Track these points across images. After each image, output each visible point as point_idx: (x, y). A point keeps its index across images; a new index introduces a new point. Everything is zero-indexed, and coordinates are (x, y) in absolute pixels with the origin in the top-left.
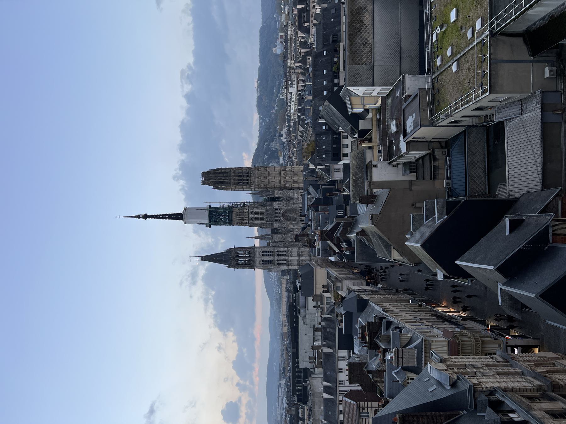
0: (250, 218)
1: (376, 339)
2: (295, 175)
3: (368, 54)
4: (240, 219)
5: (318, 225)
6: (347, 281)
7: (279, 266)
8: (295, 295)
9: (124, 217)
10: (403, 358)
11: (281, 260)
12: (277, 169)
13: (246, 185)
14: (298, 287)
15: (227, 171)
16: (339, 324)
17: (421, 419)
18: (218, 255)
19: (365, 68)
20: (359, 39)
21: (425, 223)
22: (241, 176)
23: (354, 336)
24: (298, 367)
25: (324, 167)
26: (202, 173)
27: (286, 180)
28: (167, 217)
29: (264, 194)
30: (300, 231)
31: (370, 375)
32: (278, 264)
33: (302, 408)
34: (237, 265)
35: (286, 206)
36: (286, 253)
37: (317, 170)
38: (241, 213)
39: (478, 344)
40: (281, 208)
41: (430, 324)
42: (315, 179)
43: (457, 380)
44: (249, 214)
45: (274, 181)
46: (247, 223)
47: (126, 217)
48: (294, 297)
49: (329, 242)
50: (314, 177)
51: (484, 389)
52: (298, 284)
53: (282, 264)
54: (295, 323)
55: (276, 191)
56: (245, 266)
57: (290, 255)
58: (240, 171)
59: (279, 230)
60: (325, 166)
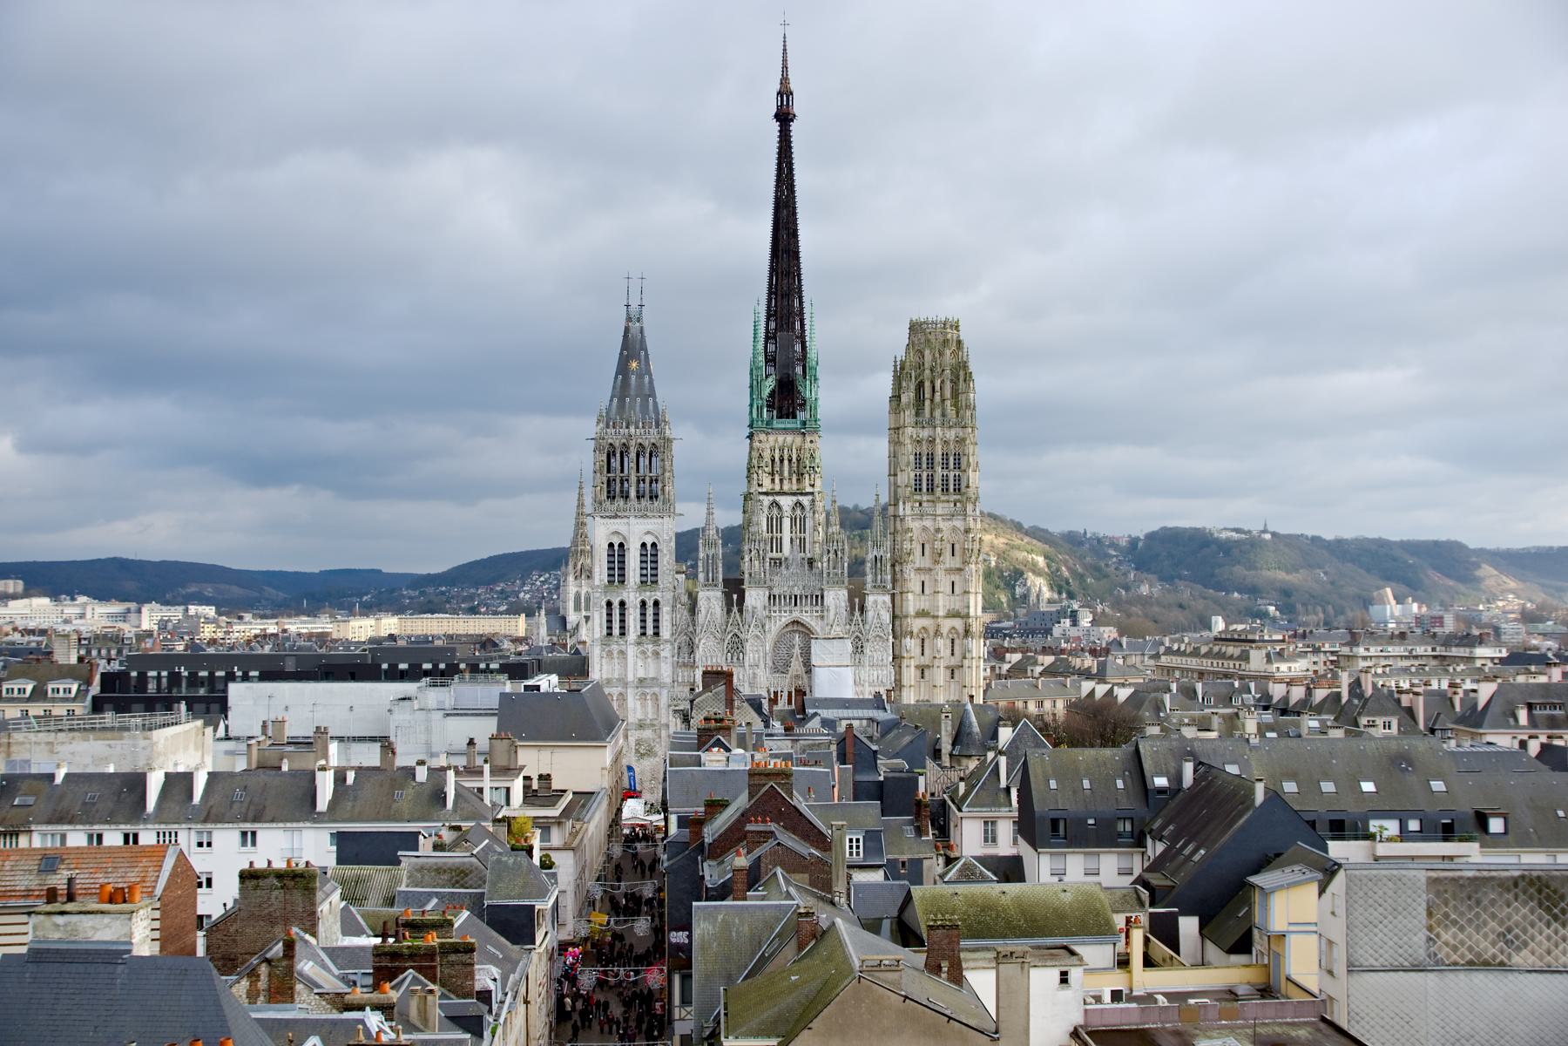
0: (778, 498)
1: (414, 977)
3: (1470, 949)
4: (773, 461)
5: (787, 757)
11: (624, 615)
14: (530, 682)
16: (430, 835)
18: (647, 379)
19: (1415, 939)
20: (1524, 917)
22: (945, 466)
24: (231, 677)
25: (1003, 784)
26: (956, 320)
27: (928, 637)
29: (875, 553)
30: (746, 691)
32: (609, 604)
36: (651, 631)
37: (990, 755)
38: (798, 467)
40: (822, 617)
42: (946, 747)
44: (794, 494)
48: (488, 665)
49: (741, 802)
50: (954, 744)
52: (548, 682)
53: (610, 621)
54: (393, 667)
55: (887, 598)
58: (964, 461)
59: (741, 611)
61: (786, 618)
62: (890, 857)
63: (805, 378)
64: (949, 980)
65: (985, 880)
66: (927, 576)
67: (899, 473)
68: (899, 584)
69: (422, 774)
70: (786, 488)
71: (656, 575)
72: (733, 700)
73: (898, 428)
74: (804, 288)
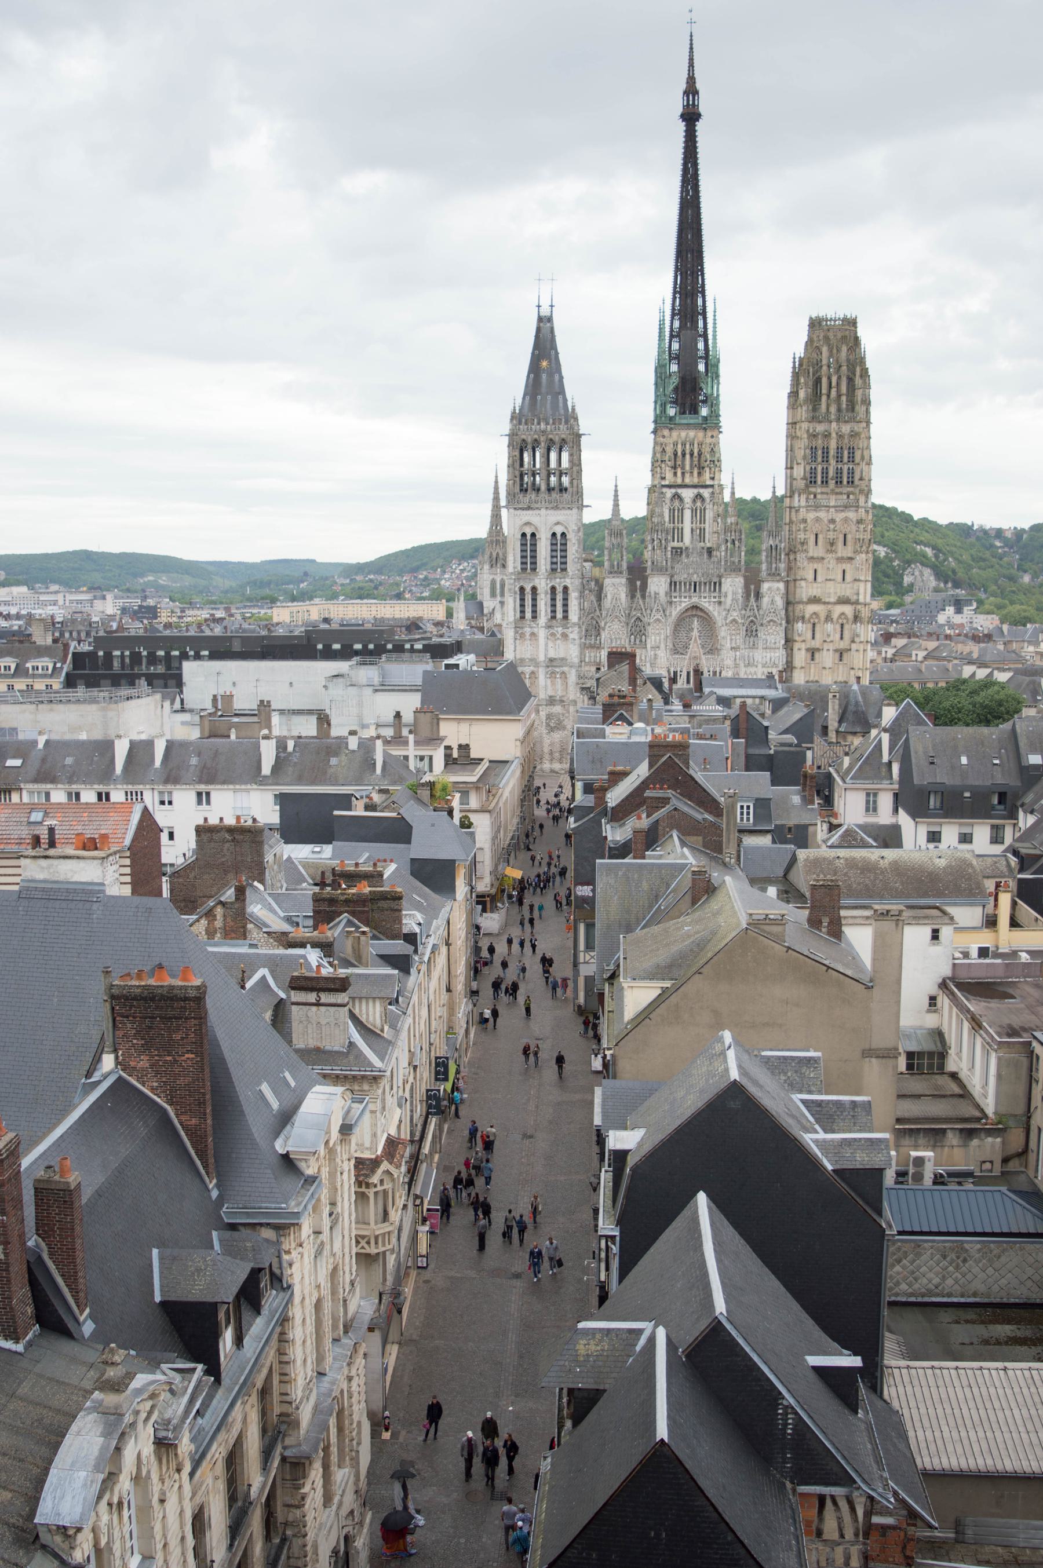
0: (680, 491)
2: (837, 655)
4: (676, 455)
5: (685, 731)
6: (488, 830)
7: (515, 593)
8: (419, 651)
9: (691, 40)
10: (318, 1004)
12: (862, 591)
13: (804, 478)
15: (857, 408)
16: (362, 797)
17: (193, 1056)
18: (557, 377)
21: (793, 1096)
22: (839, 459)
23: (331, 846)
24: (184, 656)
25: (886, 758)
27: (819, 622)
28: (687, 192)
29: (771, 542)
30: (648, 671)
31: (229, 894)
33: (54, 668)
34: (519, 447)
35: (726, 618)
36: (559, 613)
38: (699, 460)
39: (368, 1243)
40: (720, 603)
41: (407, 1095)
42: (833, 724)
43: (302, 1174)
45: (819, 578)
46: (663, 478)
47: (691, 44)
48: (412, 646)
49: (642, 771)
50: (840, 722)
51: (285, 1257)
53: (522, 606)
54: (327, 647)
55: (781, 586)
56: (517, 473)
57: (553, 634)
58: (858, 455)
60: (890, 763)
61: (685, 603)
62: (778, 822)
63: (707, 375)
64: (829, 933)
65: (865, 845)
66: (820, 565)
67: (795, 466)
68: (793, 572)
69: (353, 743)
70: (687, 480)
71: (566, 563)
72: (635, 679)
73: (795, 423)
74: (707, 287)
